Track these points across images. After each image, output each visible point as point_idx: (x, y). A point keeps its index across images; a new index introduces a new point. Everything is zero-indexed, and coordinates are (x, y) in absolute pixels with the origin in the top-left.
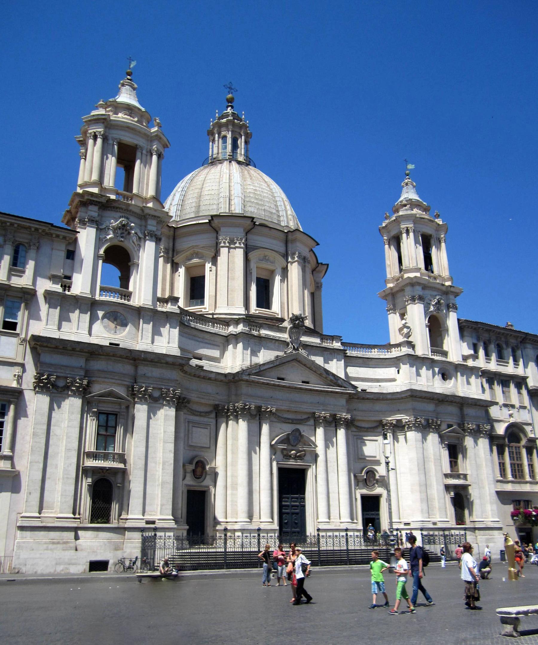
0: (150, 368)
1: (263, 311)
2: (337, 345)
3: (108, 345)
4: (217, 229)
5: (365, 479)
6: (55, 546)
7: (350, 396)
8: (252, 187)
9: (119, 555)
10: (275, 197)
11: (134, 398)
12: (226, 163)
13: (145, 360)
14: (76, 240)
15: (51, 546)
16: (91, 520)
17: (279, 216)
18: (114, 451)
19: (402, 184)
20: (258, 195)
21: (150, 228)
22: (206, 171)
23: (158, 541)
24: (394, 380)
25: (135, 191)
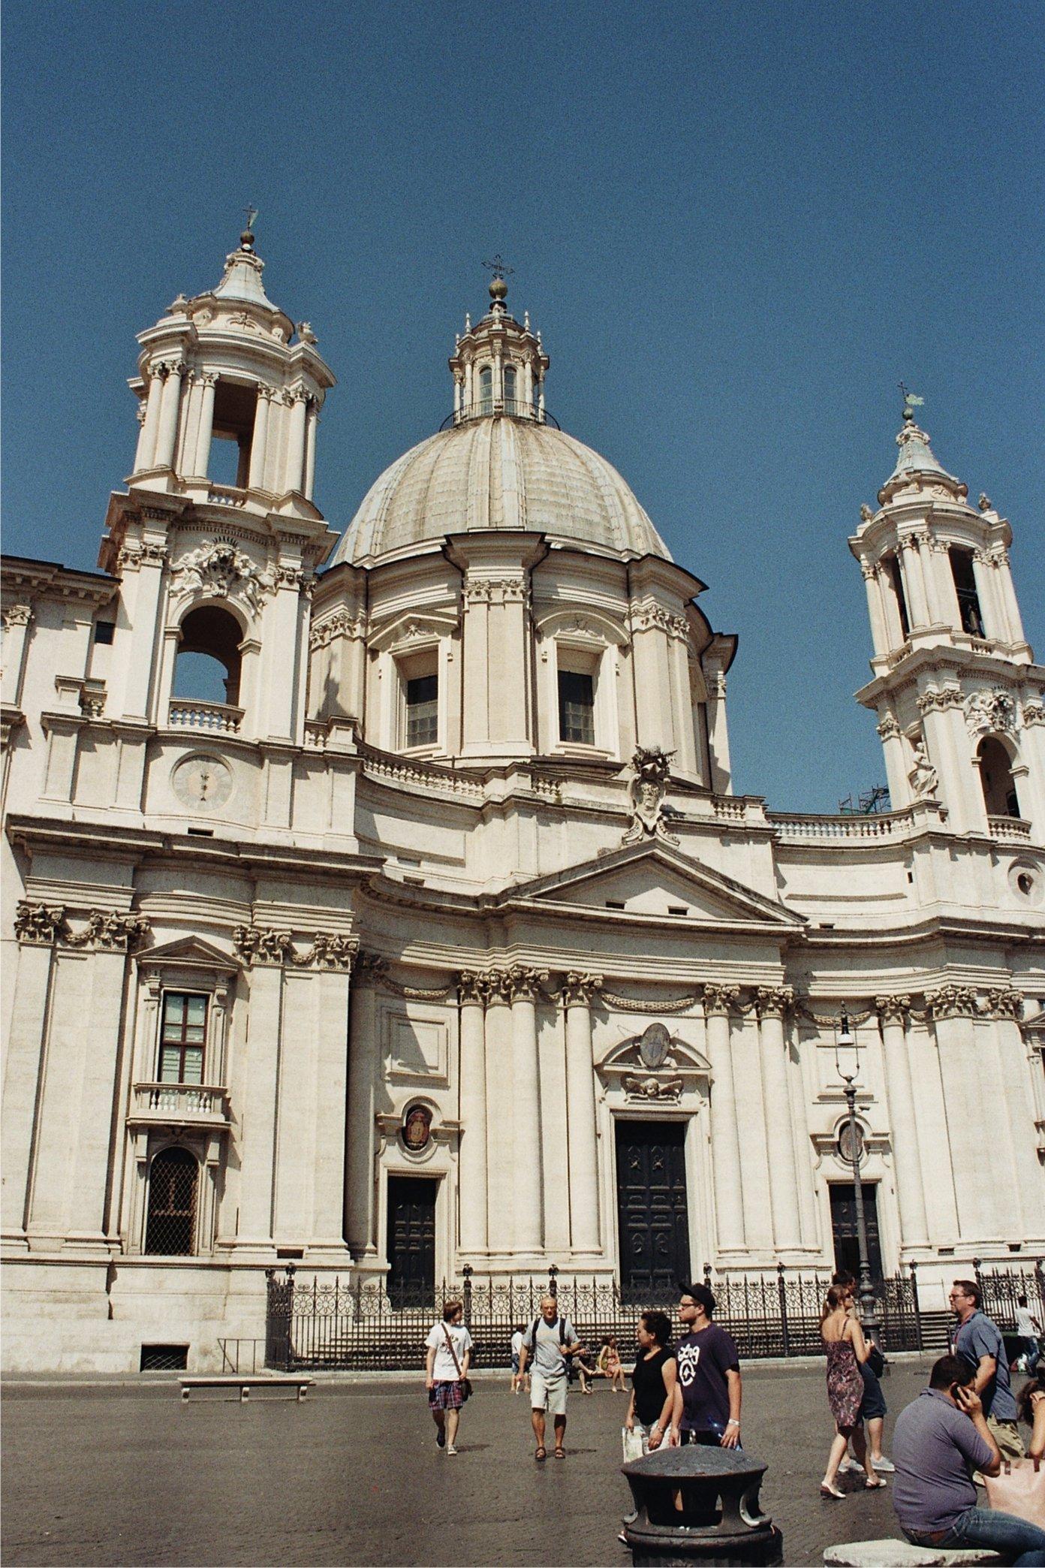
0: (286, 886)
1: (576, 749)
2: (754, 816)
3: (186, 833)
4: (462, 565)
5: (838, 1143)
6: (59, 1307)
7: (790, 941)
8: (543, 468)
9: (215, 1330)
10: (598, 488)
11: (248, 958)
12: (486, 425)
13: (272, 866)
14: (117, 598)
15: (49, 1307)
16: (147, 1246)
17: (609, 530)
18: (202, 1083)
19: (898, 438)
20: (558, 484)
21: (285, 562)
22: (441, 443)
23: (297, 1299)
24: (901, 896)
25: (253, 482)
